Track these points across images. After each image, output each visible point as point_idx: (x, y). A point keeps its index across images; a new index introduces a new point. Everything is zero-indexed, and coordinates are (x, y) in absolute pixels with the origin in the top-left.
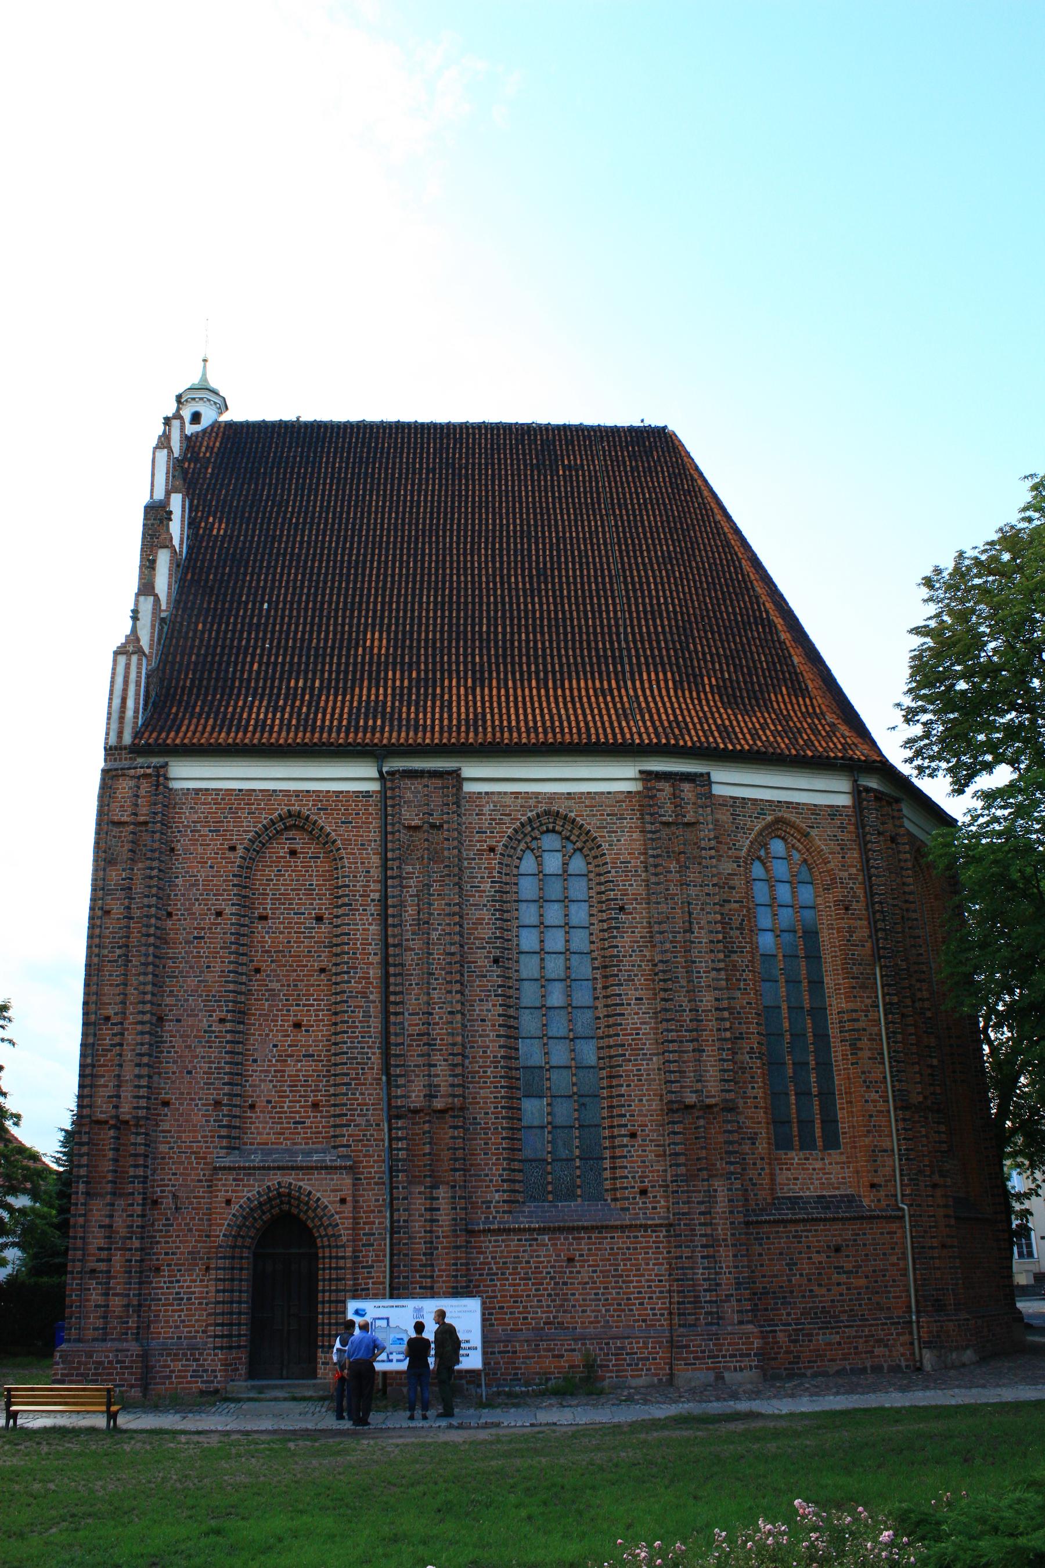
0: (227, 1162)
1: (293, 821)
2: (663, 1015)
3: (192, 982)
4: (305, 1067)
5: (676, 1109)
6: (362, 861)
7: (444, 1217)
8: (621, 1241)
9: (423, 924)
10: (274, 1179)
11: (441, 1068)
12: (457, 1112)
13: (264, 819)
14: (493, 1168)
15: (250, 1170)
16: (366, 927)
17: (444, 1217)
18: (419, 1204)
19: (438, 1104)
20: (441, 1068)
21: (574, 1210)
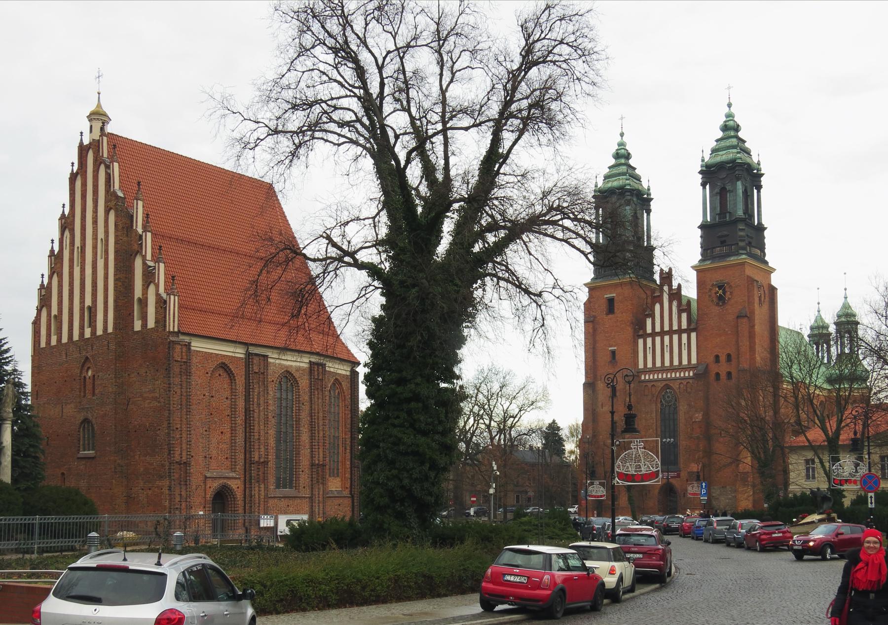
0: (208, 475)
1: (224, 366)
2: (312, 437)
3: (197, 417)
4: (225, 446)
5: (312, 465)
6: (240, 381)
7: (262, 493)
8: (299, 501)
9: (259, 404)
10: (221, 481)
11: (262, 449)
12: (266, 463)
13: (216, 363)
14: (272, 480)
15: (215, 478)
16: (241, 403)
17: (262, 493)
18: (257, 489)
19: (262, 460)
20: (262, 449)
21: (287, 491)
